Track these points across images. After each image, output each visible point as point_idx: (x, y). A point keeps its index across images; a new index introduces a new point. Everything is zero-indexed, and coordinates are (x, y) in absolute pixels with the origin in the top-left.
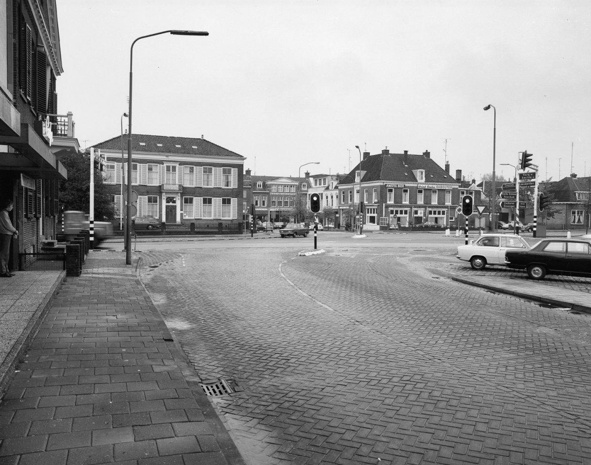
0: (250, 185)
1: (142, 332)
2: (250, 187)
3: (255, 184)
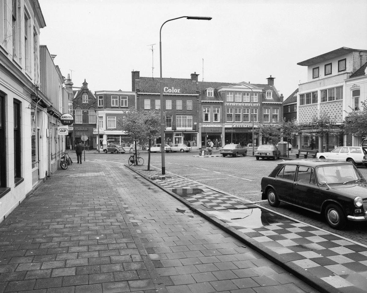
0: (198, 92)
1: (115, 242)
2: (198, 95)
3: (204, 92)
